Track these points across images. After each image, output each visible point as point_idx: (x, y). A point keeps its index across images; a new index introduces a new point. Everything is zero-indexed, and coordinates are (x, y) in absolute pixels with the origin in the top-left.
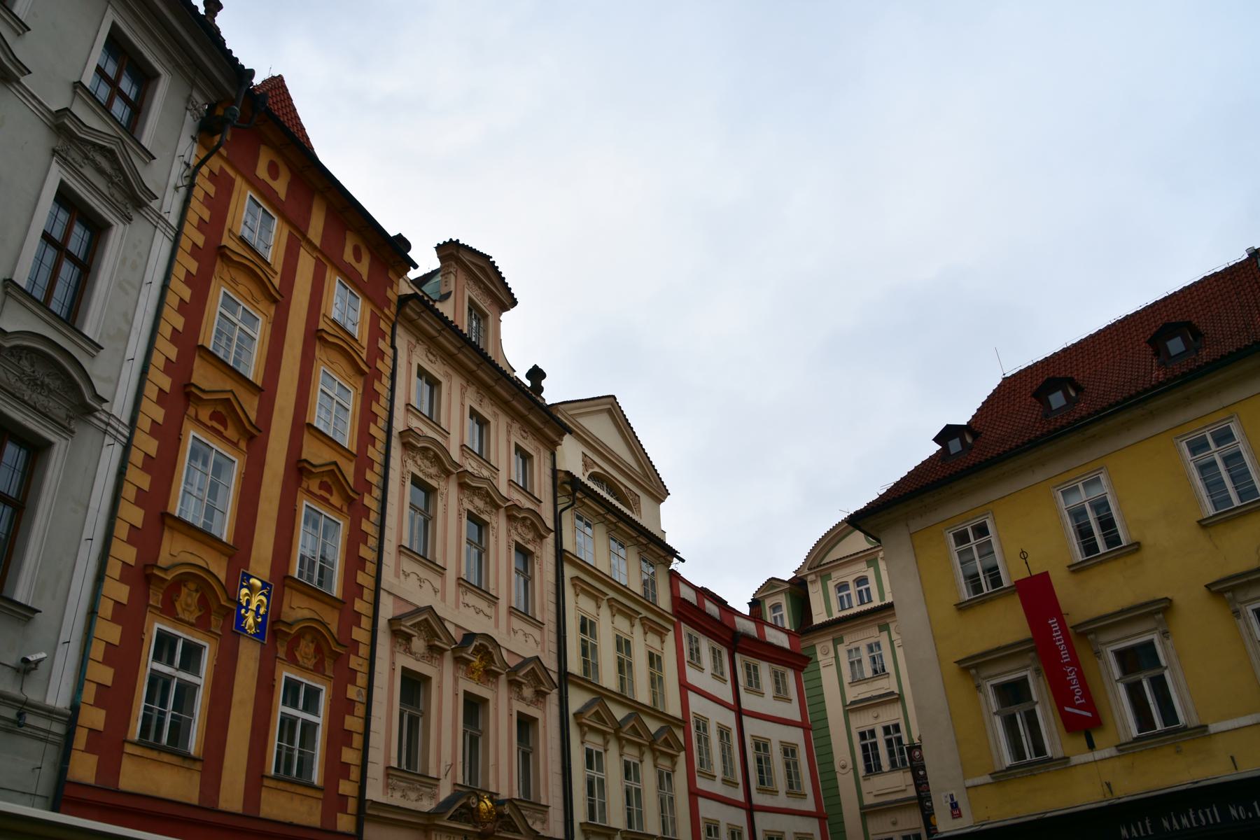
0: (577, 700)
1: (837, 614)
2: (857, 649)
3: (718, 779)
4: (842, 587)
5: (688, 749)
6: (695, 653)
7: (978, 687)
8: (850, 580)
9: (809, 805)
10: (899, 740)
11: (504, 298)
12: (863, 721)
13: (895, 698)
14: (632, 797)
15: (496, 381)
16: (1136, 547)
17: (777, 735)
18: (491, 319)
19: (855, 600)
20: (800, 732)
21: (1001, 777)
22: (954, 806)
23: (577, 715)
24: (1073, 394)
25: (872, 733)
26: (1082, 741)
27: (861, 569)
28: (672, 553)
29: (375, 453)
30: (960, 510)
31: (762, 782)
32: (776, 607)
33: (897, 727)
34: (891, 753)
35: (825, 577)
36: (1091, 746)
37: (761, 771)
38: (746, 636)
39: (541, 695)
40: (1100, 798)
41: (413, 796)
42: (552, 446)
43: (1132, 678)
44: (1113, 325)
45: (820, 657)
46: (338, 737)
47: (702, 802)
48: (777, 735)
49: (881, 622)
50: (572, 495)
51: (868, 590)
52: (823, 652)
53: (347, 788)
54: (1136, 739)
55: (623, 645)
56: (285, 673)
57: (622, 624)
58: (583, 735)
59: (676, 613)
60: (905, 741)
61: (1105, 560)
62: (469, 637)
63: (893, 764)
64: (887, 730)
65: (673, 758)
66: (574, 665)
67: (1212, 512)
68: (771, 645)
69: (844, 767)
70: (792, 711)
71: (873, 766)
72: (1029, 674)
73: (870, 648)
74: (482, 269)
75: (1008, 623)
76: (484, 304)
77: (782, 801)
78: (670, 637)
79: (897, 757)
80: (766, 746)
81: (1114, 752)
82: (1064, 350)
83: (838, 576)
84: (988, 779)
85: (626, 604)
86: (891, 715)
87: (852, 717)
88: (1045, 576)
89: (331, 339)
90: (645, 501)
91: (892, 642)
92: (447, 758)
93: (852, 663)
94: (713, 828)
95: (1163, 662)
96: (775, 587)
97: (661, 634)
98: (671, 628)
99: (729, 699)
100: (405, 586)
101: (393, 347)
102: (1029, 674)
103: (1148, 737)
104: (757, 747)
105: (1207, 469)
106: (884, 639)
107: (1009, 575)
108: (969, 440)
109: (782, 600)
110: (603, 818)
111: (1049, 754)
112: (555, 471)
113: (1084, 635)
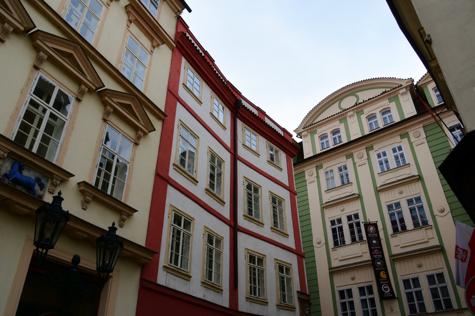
2: (331, 171)
20: (288, 193)
25: (339, 221)
27: (336, 125)
34: (352, 233)
45: (307, 177)
47: (171, 191)
49: (347, 152)
51: (340, 137)
63: (354, 240)
64: (349, 218)
71: (338, 238)
73: (340, 170)
77: (266, 231)
83: (320, 131)
91: (354, 164)
93: (327, 180)
106: (349, 163)
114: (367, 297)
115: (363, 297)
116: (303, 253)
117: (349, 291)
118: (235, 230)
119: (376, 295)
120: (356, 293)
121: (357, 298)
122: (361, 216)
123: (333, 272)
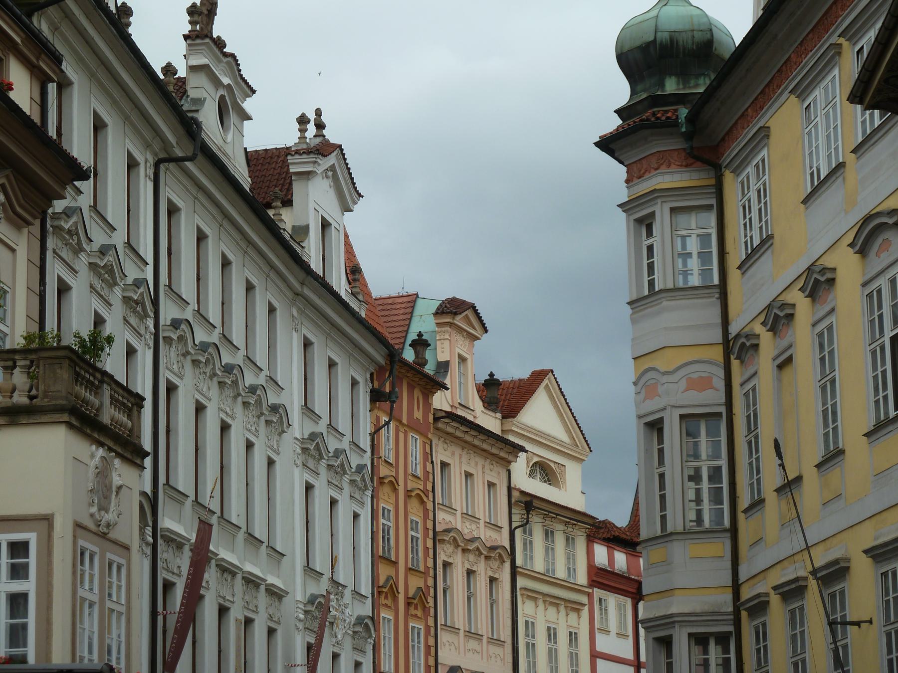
55: (552, 635)
57: (552, 611)
59: (593, 583)
78: (585, 612)
98: (584, 599)
101: (432, 462)
112: (509, 488)
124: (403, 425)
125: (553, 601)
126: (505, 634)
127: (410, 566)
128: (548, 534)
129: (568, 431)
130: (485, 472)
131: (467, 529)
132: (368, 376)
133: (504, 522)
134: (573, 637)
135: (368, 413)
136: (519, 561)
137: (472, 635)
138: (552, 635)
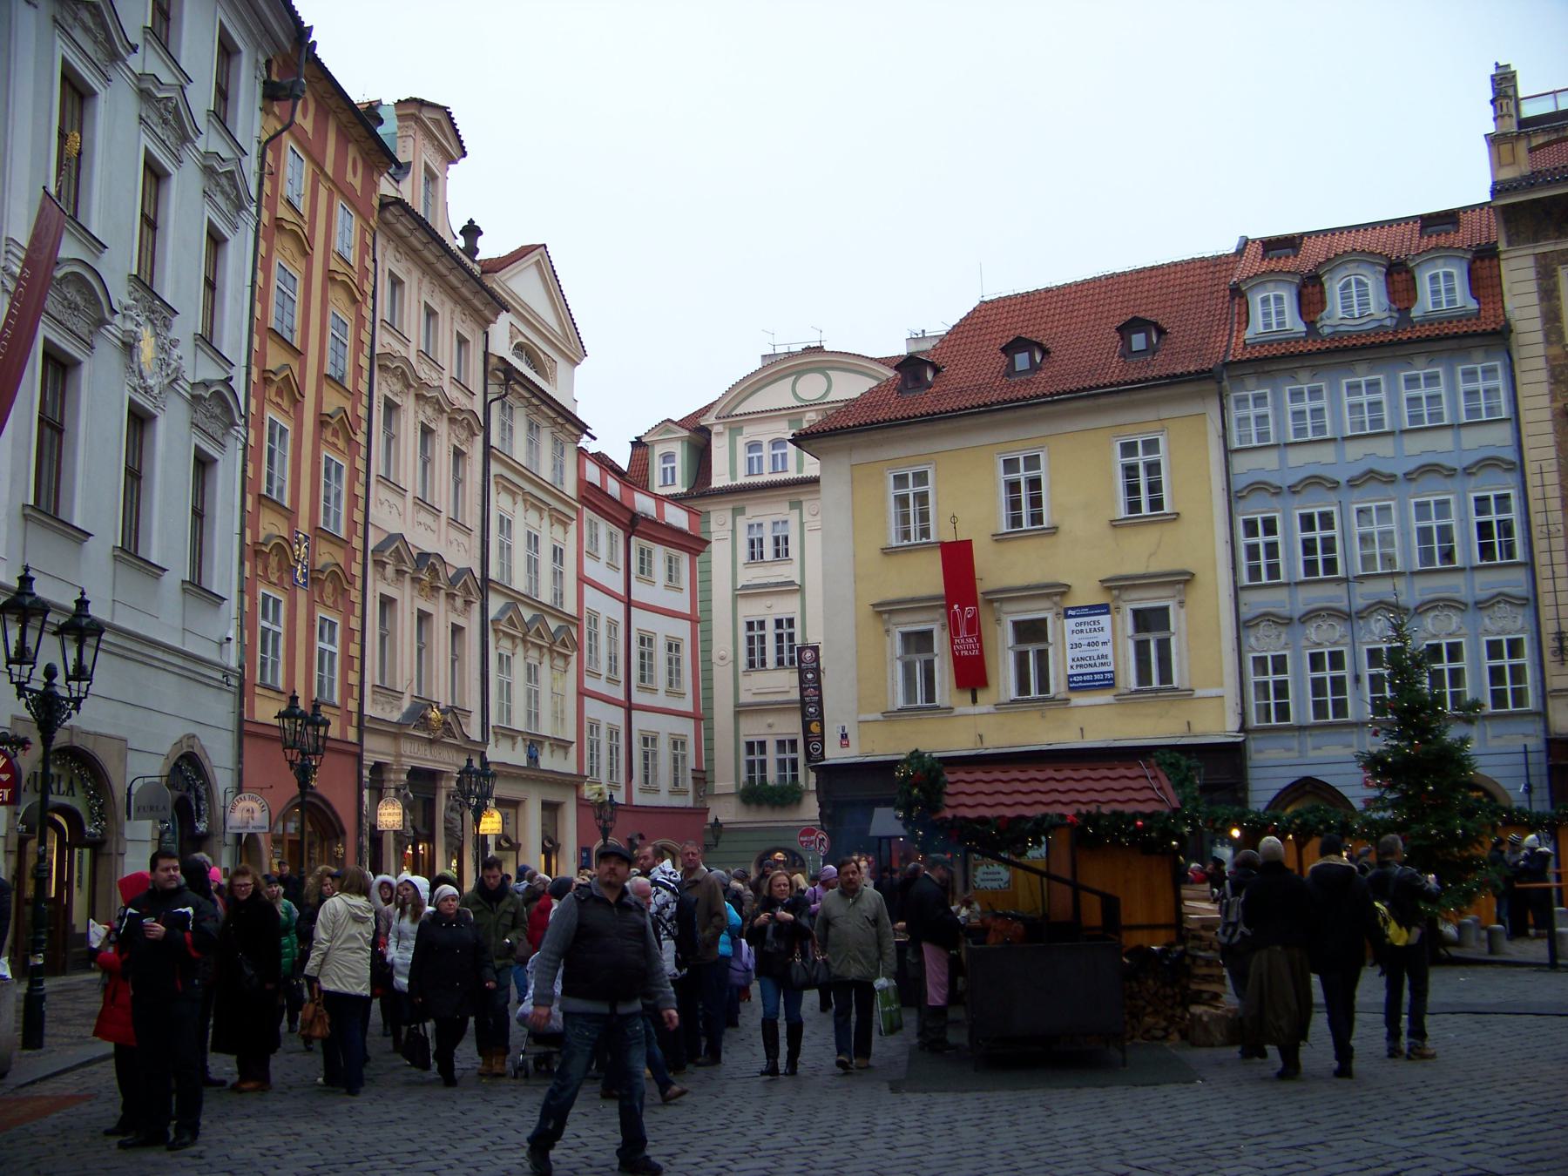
0: (496, 604)
1: (742, 479)
2: (760, 525)
3: (603, 678)
4: (754, 446)
5: (578, 647)
6: (595, 538)
7: (887, 631)
8: (765, 440)
9: (687, 705)
10: (791, 636)
11: (454, 151)
12: (753, 609)
13: (793, 588)
14: (533, 697)
15: (463, 282)
16: (1054, 530)
17: (663, 628)
18: (440, 180)
19: (767, 465)
21: (891, 716)
22: (844, 736)
23: (496, 621)
24: (1038, 359)
25: (762, 624)
26: (969, 696)
28: (583, 428)
29: (364, 388)
30: (903, 454)
31: (643, 678)
32: (668, 457)
33: (791, 622)
34: (780, 650)
35: (735, 430)
36: (974, 700)
37: (642, 667)
38: (647, 519)
39: (468, 603)
40: (971, 746)
41: (388, 708)
42: (485, 323)
43: (1023, 647)
44: (1099, 279)
45: (713, 527)
46: (348, 660)
48: (663, 628)
50: (506, 383)
52: (725, 533)
53: (352, 705)
54: (1013, 701)
55: (533, 541)
56: (320, 613)
57: (533, 516)
58: (498, 641)
59: (583, 499)
60: (798, 641)
61: (1027, 535)
62: (424, 556)
63: (780, 662)
64: (779, 623)
65: (566, 657)
66: (493, 573)
67: (1123, 515)
68: (670, 528)
69: (722, 658)
70: (681, 603)
71: (755, 662)
72: (936, 628)
74: (437, 122)
75: (928, 577)
76: (436, 163)
77: (660, 700)
78: (573, 527)
79: (786, 655)
80: (650, 640)
81: (992, 709)
82: (1048, 290)
83: (750, 432)
84: (879, 716)
85: (541, 497)
86: (786, 607)
87: (741, 604)
88: (967, 545)
89: (339, 278)
90: (562, 364)
91: (802, 524)
92: (407, 674)
94: (595, 726)
95: (1050, 639)
96: (669, 431)
97: (561, 520)
98: (574, 515)
99: (621, 591)
100: (389, 515)
101: (374, 260)
102: (936, 628)
103: (1023, 701)
104: (642, 643)
105: (1130, 471)
106: (793, 517)
107: (938, 533)
108: (930, 376)
109: (679, 450)
110: (509, 721)
111: (938, 702)
112: (486, 354)
113: (991, 601)
114: (788, 755)
115: (782, 756)
116: (701, 717)
117: (762, 744)
118: (629, 707)
119: (800, 755)
120: (771, 748)
121: (772, 755)
122: (797, 623)
123: (741, 710)
124: (326, 175)
125: (536, 505)
126: (474, 521)
127: (329, 370)
128: (533, 427)
129: (561, 325)
130: (451, 321)
131: (424, 372)
132: (262, 60)
133: (477, 387)
134: (558, 554)
135: (258, 114)
136: (494, 441)
137: (422, 503)
138: (533, 541)
